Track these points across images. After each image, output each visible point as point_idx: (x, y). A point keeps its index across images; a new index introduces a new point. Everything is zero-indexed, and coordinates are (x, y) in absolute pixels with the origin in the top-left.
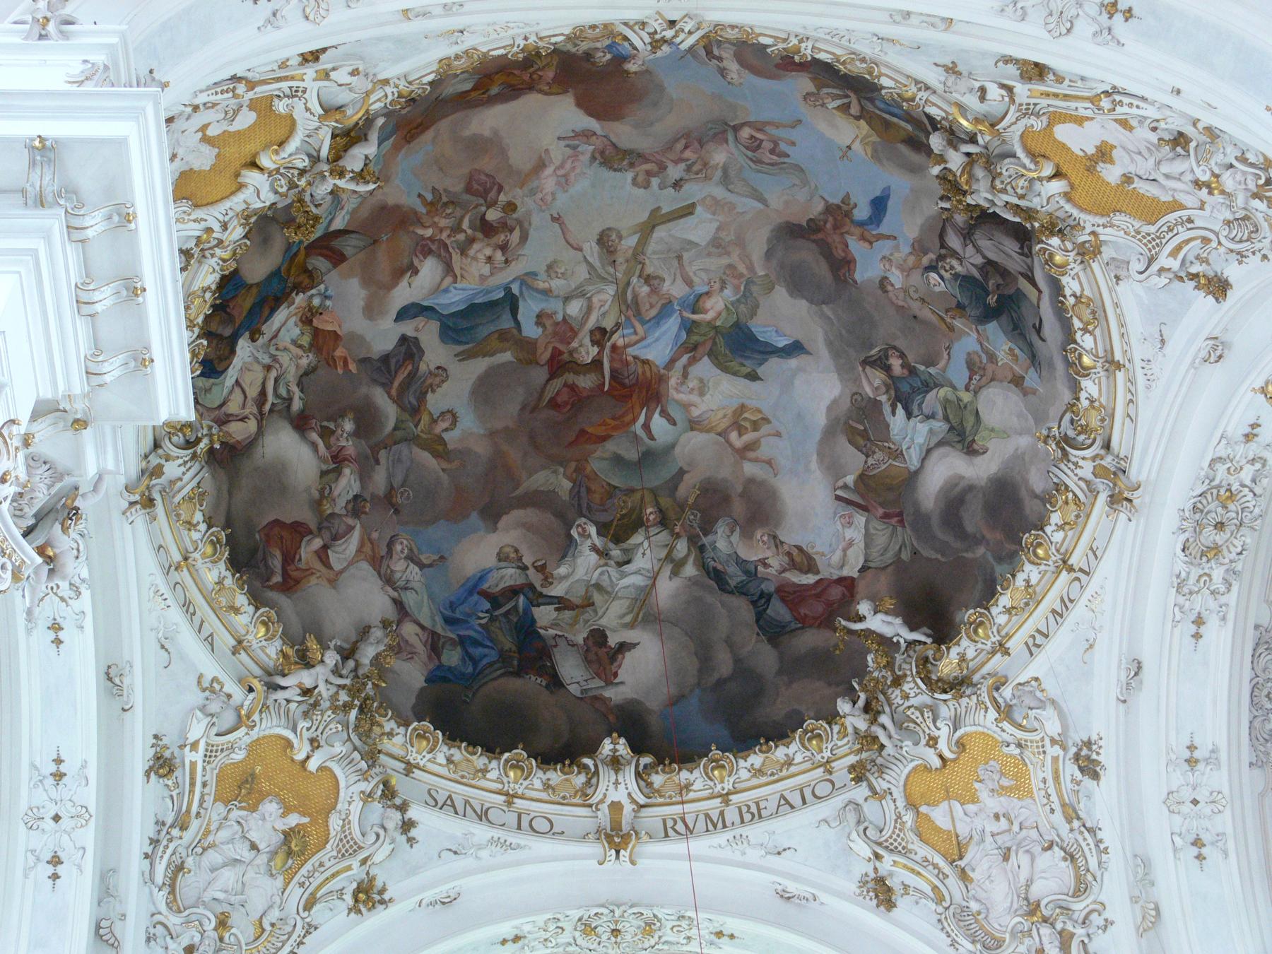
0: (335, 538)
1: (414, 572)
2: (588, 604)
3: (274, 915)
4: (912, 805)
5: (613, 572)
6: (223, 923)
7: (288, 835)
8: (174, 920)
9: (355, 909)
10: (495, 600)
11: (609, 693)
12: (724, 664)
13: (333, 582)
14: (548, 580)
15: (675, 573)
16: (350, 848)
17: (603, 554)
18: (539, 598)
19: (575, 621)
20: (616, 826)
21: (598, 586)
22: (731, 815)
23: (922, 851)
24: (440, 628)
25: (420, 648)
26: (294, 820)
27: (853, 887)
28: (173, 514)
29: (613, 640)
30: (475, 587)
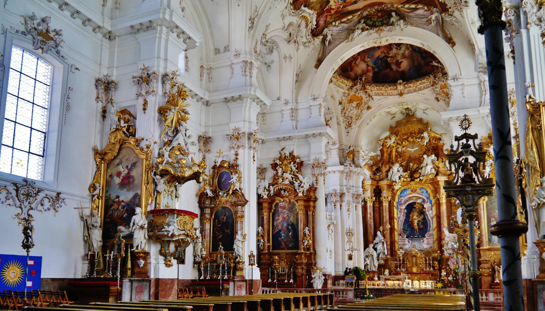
0: (356, 60)
1: (369, 59)
2: (395, 56)
3: (357, 114)
4: (441, 89)
5: (398, 51)
6: (351, 118)
7: (357, 104)
8: (346, 119)
9: (367, 110)
10: (381, 59)
11: (400, 70)
12: (416, 63)
13: (357, 66)
14: (389, 54)
15: (408, 50)
16: (366, 103)
17: (397, 49)
18: (388, 57)
19: (393, 60)
20: (401, 92)
21: (397, 54)
22: (417, 89)
23: (443, 94)
24: (374, 66)
25: (371, 70)
26: (358, 102)
27: (434, 98)
28: (335, 78)
29: (400, 61)
30: (378, 58)
